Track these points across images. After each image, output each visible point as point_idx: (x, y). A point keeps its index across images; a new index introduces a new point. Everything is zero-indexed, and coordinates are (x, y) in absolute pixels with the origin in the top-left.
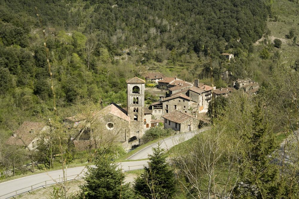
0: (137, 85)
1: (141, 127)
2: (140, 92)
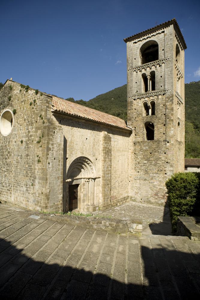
0: (152, 39)
1: (163, 158)
2: (161, 53)
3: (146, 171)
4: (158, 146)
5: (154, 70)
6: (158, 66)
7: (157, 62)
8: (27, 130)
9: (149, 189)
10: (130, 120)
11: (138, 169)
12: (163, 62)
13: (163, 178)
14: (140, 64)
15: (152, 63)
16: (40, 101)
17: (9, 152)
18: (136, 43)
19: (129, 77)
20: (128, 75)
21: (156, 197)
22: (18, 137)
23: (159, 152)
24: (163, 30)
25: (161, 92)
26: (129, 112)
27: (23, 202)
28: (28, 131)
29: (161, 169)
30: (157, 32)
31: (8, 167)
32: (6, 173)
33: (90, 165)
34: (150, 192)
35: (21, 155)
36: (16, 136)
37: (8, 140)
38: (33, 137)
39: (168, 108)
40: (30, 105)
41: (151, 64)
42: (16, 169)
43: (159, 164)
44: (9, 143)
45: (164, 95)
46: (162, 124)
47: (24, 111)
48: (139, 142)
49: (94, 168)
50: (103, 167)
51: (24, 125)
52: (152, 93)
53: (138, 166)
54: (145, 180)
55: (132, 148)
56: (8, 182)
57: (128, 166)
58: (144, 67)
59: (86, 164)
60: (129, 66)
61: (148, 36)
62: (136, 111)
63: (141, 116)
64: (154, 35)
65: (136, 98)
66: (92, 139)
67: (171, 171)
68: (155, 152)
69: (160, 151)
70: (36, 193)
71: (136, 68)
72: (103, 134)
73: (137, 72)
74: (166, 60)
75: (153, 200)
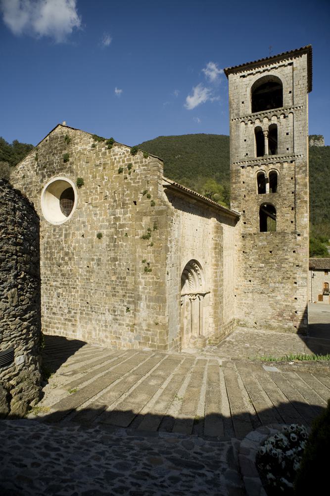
0: (272, 73)
1: (291, 260)
2: (286, 97)
3: (263, 279)
4: (283, 241)
5: (276, 123)
6: (282, 116)
7: (280, 111)
8: (111, 216)
9: (269, 307)
10: (235, 199)
11: (249, 276)
12: (290, 111)
13: (292, 290)
14: (250, 111)
15: (273, 112)
16: (143, 166)
17: (67, 254)
18: (244, 76)
19: (232, 131)
20: (231, 127)
21: (280, 319)
22: (89, 228)
23: (284, 250)
24: (290, 61)
25: (287, 158)
26: (234, 187)
27: (105, 340)
28: (114, 218)
29: (288, 276)
30: (281, 63)
31: (66, 280)
32: (60, 291)
33: (198, 272)
34: (270, 311)
35: (99, 260)
36: (84, 226)
37: (64, 232)
38: (127, 229)
39: (298, 183)
40: (117, 172)
41: (270, 112)
42: (88, 282)
43: (284, 268)
44: (66, 237)
45: (292, 162)
46: (290, 206)
47: (104, 182)
48: (250, 234)
49: (202, 278)
50: (215, 275)
51: (105, 207)
52: (273, 158)
53: (251, 271)
54: (261, 293)
55: (240, 244)
56: (66, 306)
57: (234, 272)
58: (259, 116)
59: (193, 271)
60: (233, 113)
61: (265, 68)
62: (245, 185)
63: (253, 193)
64: (275, 68)
65: (246, 165)
66: (202, 230)
67: (303, 278)
68: (278, 250)
69: (285, 248)
70: (141, 323)
71: (245, 118)
72: (213, 221)
73: (246, 124)
74: (296, 109)
75: (274, 323)
